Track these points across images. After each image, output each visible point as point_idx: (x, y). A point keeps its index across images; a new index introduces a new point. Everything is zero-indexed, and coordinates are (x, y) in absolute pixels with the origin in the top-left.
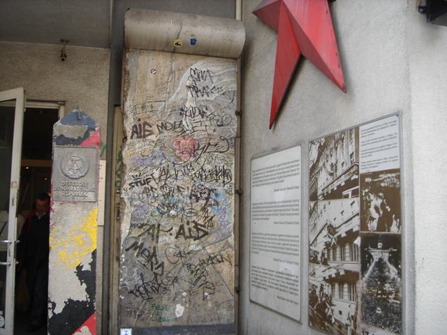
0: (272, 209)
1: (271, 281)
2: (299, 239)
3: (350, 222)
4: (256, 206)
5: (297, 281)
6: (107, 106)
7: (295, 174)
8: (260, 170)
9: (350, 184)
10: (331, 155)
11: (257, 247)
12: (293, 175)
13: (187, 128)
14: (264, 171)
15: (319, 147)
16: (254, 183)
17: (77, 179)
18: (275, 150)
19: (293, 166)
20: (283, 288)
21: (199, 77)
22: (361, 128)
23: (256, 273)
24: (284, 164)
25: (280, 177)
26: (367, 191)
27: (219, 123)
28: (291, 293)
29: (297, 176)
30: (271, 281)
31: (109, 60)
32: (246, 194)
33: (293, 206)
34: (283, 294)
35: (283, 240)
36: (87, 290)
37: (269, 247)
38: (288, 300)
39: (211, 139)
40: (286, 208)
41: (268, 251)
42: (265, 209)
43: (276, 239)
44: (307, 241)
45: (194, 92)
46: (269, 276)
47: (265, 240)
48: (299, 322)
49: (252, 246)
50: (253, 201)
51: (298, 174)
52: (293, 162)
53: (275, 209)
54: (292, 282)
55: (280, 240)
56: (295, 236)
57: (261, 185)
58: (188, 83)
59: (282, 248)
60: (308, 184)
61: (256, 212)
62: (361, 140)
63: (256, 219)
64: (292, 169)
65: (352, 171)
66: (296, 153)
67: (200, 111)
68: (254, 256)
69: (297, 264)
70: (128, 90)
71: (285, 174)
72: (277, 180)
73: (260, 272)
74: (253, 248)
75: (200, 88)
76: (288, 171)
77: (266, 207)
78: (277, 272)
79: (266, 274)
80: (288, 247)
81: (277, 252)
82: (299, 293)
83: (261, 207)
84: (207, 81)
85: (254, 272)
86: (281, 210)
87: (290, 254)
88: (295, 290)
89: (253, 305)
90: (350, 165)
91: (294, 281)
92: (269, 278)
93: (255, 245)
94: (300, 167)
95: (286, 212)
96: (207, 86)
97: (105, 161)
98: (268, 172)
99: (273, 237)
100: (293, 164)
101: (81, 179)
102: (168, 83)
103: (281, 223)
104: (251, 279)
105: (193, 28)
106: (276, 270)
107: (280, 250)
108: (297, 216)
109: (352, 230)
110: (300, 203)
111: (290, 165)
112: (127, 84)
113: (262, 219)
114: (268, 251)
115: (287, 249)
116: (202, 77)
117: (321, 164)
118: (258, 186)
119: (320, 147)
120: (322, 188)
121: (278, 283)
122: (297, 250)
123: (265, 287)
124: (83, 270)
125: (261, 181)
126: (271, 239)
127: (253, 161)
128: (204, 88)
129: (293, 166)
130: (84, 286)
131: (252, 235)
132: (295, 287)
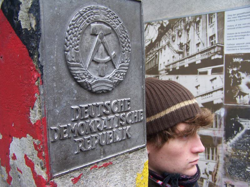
3: (211, 95)
9: (206, 63)
10: (180, 36)
15: (159, 28)
17: (108, 92)
22: (226, 14)
26: (235, 69)
62: (226, 23)
65: (212, 51)
90: (209, 46)
109: (212, 102)
117: (163, 43)
119: (162, 27)
120: (166, 64)
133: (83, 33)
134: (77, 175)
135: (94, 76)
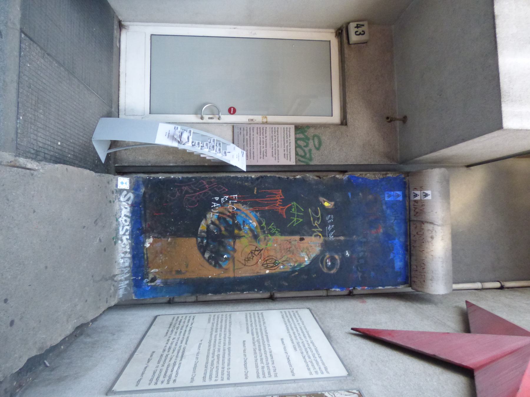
0: (260, 337)
1: (175, 341)
2: (226, 382)
4: (260, 316)
5: (168, 383)
6: (347, 164)
7: (309, 369)
8: (301, 319)
11: (216, 320)
12: (308, 366)
14: (301, 324)
16: (285, 312)
18: (328, 336)
19: (318, 363)
20: (163, 358)
23: (187, 321)
24: (317, 351)
25: (299, 346)
28: (154, 373)
30: (175, 341)
31: (389, 163)
32: (271, 305)
33: (268, 367)
34: (156, 358)
35: (224, 354)
37: (216, 336)
40: (263, 356)
41: (211, 335)
42: (258, 327)
43: (225, 345)
46: (181, 339)
47: (223, 330)
49: (217, 314)
50: (265, 313)
51: (311, 373)
52: (323, 364)
55: (224, 350)
56: (229, 375)
57: (285, 321)
59: (213, 354)
60: (300, 391)
61: (254, 317)
63: (246, 317)
64: (314, 362)
66: (337, 369)
68: (206, 317)
69: (192, 380)
71: (305, 353)
72: (295, 341)
73: (187, 326)
74: (214, 316)
76: (309, 358)
77: (261, 329)
78: (184, 349)
79: (184, 334)
80: (215, 362)
81: (210, 346)
82: (152, 387)
83: (260, 322)
85: (187, 319)
86: (260, 350)
87: (206, 367)
88: (157, 379)
89: (150, 319)
91: (170, 377)
92: (178, 338)
93: (218, 318)
94: (320, 375)
95: (258, 357)
97: (294, 164)
98: (301, 330)
99: (227, 340)
100: (320, 364)
103: (244, 351)
105: (440, 238)
106: (187, 347)
107: (211, 351)
110: (273, 379)
111: (319, 360)
113: (247, 324)
114: (211, 335)
115: (213, 361)
122: (210, 378)
123: (169, 333)
125: (288, 320)
126: (225, 338)
127: (307, 311)
129: (318, 363)
131: (228, 314)
132: (161, 378)
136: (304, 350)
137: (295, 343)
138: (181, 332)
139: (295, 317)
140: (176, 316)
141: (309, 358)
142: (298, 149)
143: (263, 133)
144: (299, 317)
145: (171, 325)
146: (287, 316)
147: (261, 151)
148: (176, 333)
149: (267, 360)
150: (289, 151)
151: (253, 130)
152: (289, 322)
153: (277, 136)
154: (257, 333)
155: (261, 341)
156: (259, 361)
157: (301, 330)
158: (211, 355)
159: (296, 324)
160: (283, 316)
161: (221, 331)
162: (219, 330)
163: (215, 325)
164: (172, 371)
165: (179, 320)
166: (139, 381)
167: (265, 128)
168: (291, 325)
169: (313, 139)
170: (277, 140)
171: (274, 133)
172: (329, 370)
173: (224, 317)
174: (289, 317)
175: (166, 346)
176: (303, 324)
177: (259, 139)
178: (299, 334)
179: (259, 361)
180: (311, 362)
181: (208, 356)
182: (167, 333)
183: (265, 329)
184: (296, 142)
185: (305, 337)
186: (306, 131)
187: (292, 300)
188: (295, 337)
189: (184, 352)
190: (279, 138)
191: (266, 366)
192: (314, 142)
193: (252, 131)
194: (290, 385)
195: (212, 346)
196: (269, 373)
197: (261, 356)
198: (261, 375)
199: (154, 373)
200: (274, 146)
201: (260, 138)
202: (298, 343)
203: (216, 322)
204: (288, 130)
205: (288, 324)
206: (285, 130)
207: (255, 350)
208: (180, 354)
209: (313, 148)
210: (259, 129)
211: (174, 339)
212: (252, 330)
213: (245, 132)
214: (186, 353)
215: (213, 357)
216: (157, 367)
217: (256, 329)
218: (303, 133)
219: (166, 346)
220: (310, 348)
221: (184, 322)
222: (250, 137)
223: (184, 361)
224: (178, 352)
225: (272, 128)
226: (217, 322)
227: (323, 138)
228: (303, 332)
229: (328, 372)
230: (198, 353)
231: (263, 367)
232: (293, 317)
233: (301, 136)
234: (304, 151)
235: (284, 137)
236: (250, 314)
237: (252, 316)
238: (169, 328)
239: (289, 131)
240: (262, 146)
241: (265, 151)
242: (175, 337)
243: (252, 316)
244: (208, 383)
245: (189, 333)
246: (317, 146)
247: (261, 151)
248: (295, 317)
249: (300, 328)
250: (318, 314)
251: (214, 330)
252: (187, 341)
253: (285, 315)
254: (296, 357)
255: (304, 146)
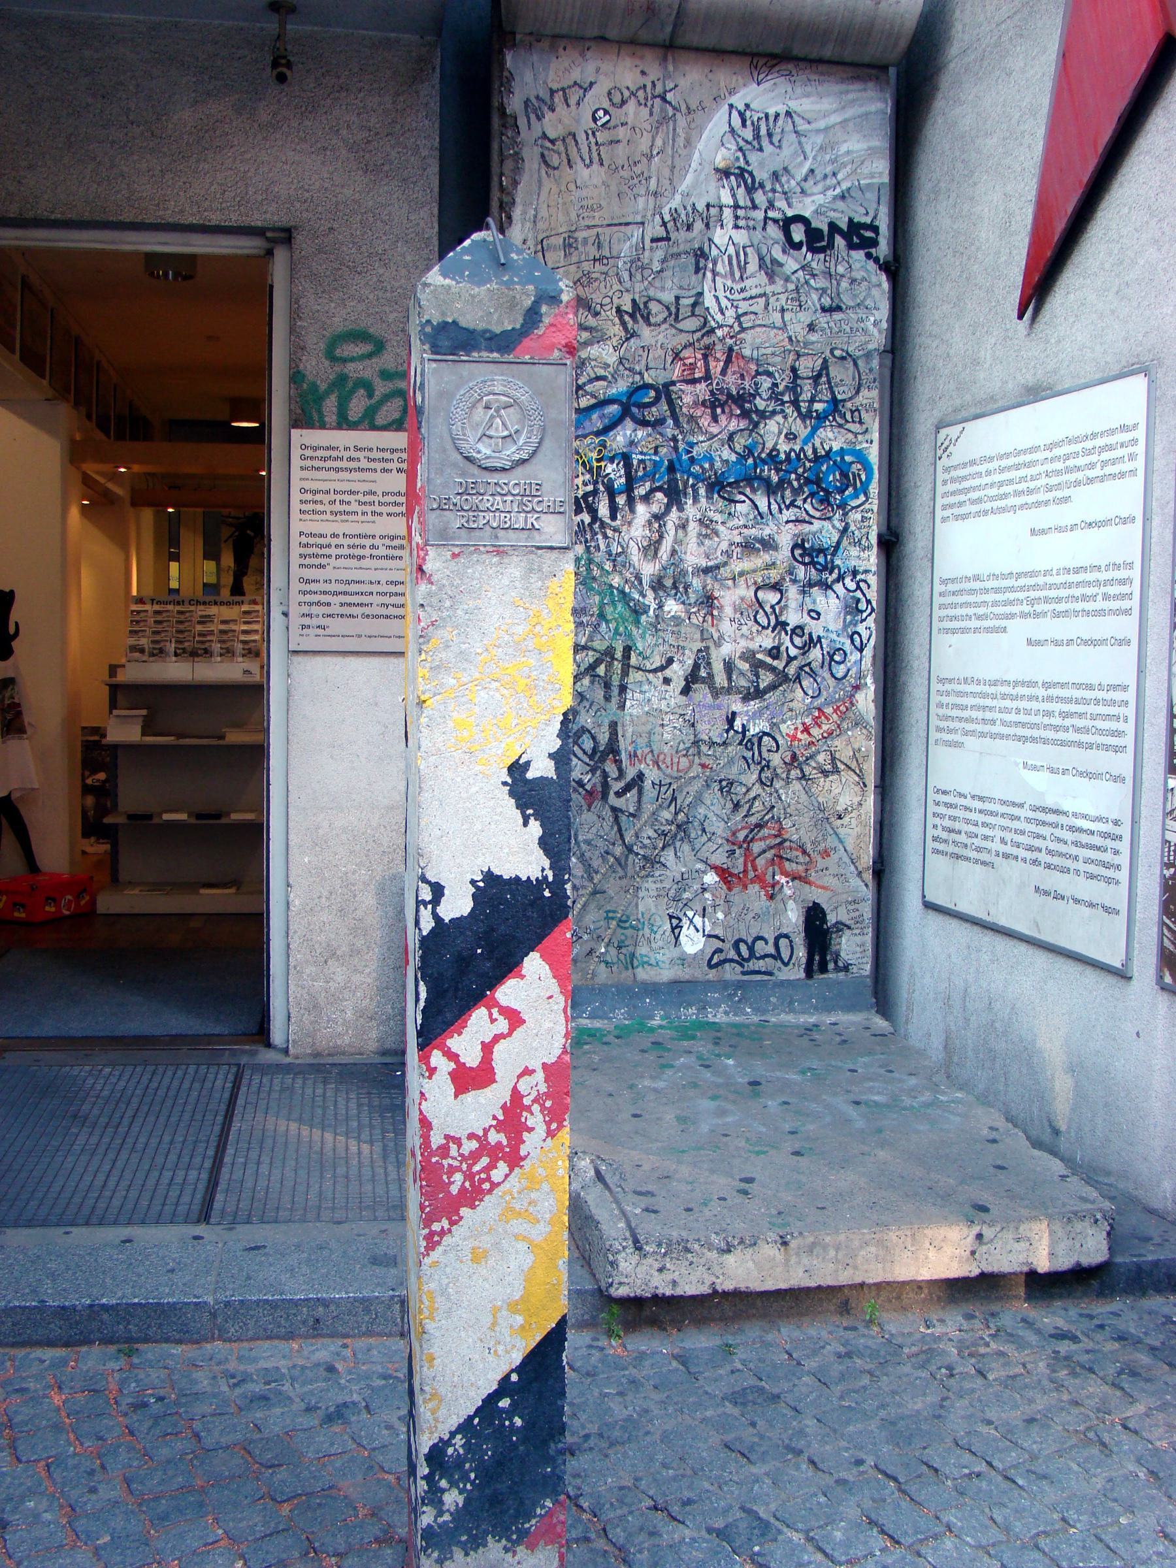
0: (1021, 595)
1: (1008, 836)
2: (1131, 696)
4: (951, 587)
7: (1122, 475)
8: (973, 463)
11: (952, 725)
12: (1113, 476)
13: (719, 317)
14: (991, 466)
16: (944, 507)
17: (504, 470)
18: (1035, 393)
19: (1110, 448)
20: (1056, 861)
21: (757, 136)
23: (951, 812)
27: (827, 301)
28: (1092, 877)
29: (1128, 480)
30: (1008, 836)
32: (915, 546)
33: (1106, 583)
35: (1060, 699)
36: (543, 842)
38: (1077, 901)
39: (798, 355)
40: (1077, 592)
41: (1002, 737)
42: (990, 597)
44: (1163, 704)
45: (741, 192)
47: (988, 702)
48: (1122, 975)
51: (1133, 472)
52: (1112, 432)
53: (1033, 594)
54: (1097, 840)
55: (1050, 699)
57: (978, 514)
58: (722, 158)
59: (1056, 728)
61: (954, 606)
63: (954, 631)
64: (1105, 456)
66: (1127, 399)
67: (761, 259)
68: (941, 757)
69: (1118, 779)
70: (515, 183)
71: (1079, 475)
72: (1041, 497)
73: (966, 808)
75: (762, 175)
76: (1091, 466)
77: (997, 590)
78: (1035, 809)
79: (992, 814)
80: (1080, 723)
81: (1034, 740)
82: (1123, 876)
83: (972, 592)
84: (786, 152)
85: (942, 810)
86: (1059, 600)
87: (1090, 746)
88: (1106, 865)
89: (934, 919)
91: (1106, 835)
93: (947, 718)
94: (1140, 449)
95: (1079, 606)
96: (785, 169)
98: (1009, 468)
101: (519, 471)
102: (650, 157)
103: (1056, 643)
104: (931, 832)
106: (1030, 801)
107: (1050, 734)
108: (1122, 618)
110: (1136, 574)
111: (1100, 442)
112: (509, 165)
113: (976, 630)
114: (1002, 737)
115: (1078, 730)
116: (770, 135)
118: (964, 517)
121: (1038, 843)
123: (984, 856)
124: (530, 775)
128: (775, 176)
129: (1110, 448)
130: (535, 829)
131: (935, 686)
132: (1107, 857)
133: (474, 406)
134: (457, 550)
135: (484, 450)
136: (1072, 477)
137: (1049, 496)
138: (984, 825)
139: (964, 478)
140: (930, 844)
141: (1091, 466)
142: (380, 421)
143: (322, 547)
144: (965, 465)
145: (958, 857)
146: (961, 504)
147: (387, 557)
148: (986, 838)
149: (1089, 584)
150: (387, 455)
151: (308, 582)
152: (979, 501)
153: (332, 497)
154: (1010, 603)
155: (1026, 595)
156: (1089, 606)
157: (1009, 468)
158: (1061, 735)
159: (988, 480)
160: (957, 517)
161: (991, 709)
162: (988, 715)
163: (970, 727)
164: (1092, 833)
165: (944, 835)
166: (1107, 910)
167: (304, 540)
168: (991, 499)
169: (344, 361)
170: (346, 498)
171: (319, 507)
172: (1130, 423)
173: (945, 700)
174: (962, 498)
175: (1024, 860)
176: (991, 459)
177: (341, 562)
178: (1023, 479)
179: (1089, 606)
180: (1105, 463)
181: (1063, 743)
182: (984, 863)
183: (996, 577)
184: (353, 426)
185: (1027, 465)
186: (314, 387)
187: (899, 478)
188: (1030, 492)
189: (1044, 810)
190: (339, 486)
191: (1103, 589)
192: (352, 360)
193: (313, 587)
194: (1154, 533)
195: (1036, 733)
196: (1122, 582)
197: (1076, 599)
198: (1125, 604)
199: (1092, 877)
200: (368, 509)
201: (338, 557)
202: (1049, 489)
203: (963, 725)
204: (309, 453)
205: (988, 506)
206: (309, 463)
207: (1057, 615)
208: (1051, 818)
209: (377, 363)
210: (308, 561)
211: (1003, 841)
212: (998, 617)
213: (315, 610)
214: (1049, 802)
215: (1066, 730)
216: (1077, 871)
217: (995, 604)
218: (320, 399)
219: (1024, 860)
220: (1067, 457)
221: (954, 819)
222: (336, 593)
223: (1066, 806)
224: (1044, 823)
225: (302, 512)
226: (960, 719)
227: (340, 321)
228: (1017, 467)
229: (1135, 426)
230: (1052, 771)
231: (1106, 597)
232: (966, 484)
233: (330, 405)
234: (386, 398)
235: (337, 470)
236: (941, 620)
237: (951, 612)
238: (967, 859)
239: (315, 449)
240: (367, 552)
241: (387, 542)
242: (997, 840)
243: (951, 612)
244: (1129, 740)
245: (991, 800)
246: (368, 348)
247: (387, 557)
248: (964, 478)
249: (1002, 470)
250: (958, 402)
251: (987, 728)
252: (1014, 804)
253: (956, 511)
254: (1090, 501)
255: (370, 396)
